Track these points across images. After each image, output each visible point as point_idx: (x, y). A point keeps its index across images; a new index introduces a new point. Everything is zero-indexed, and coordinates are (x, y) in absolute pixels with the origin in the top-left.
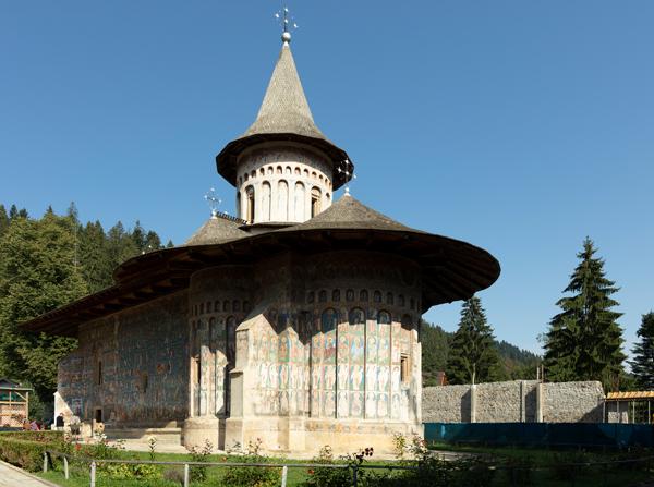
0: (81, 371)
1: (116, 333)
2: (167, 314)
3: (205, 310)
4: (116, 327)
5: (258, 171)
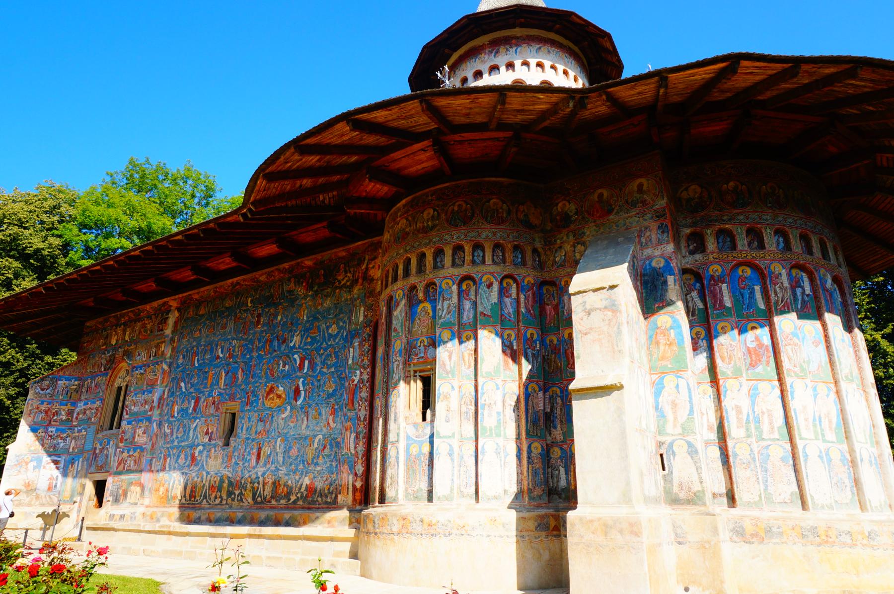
0: (74, 404)
1: (168, 331)
2: (301, 291)
3: (448, 260)
4: (171, 321)
5: (503, 69)
